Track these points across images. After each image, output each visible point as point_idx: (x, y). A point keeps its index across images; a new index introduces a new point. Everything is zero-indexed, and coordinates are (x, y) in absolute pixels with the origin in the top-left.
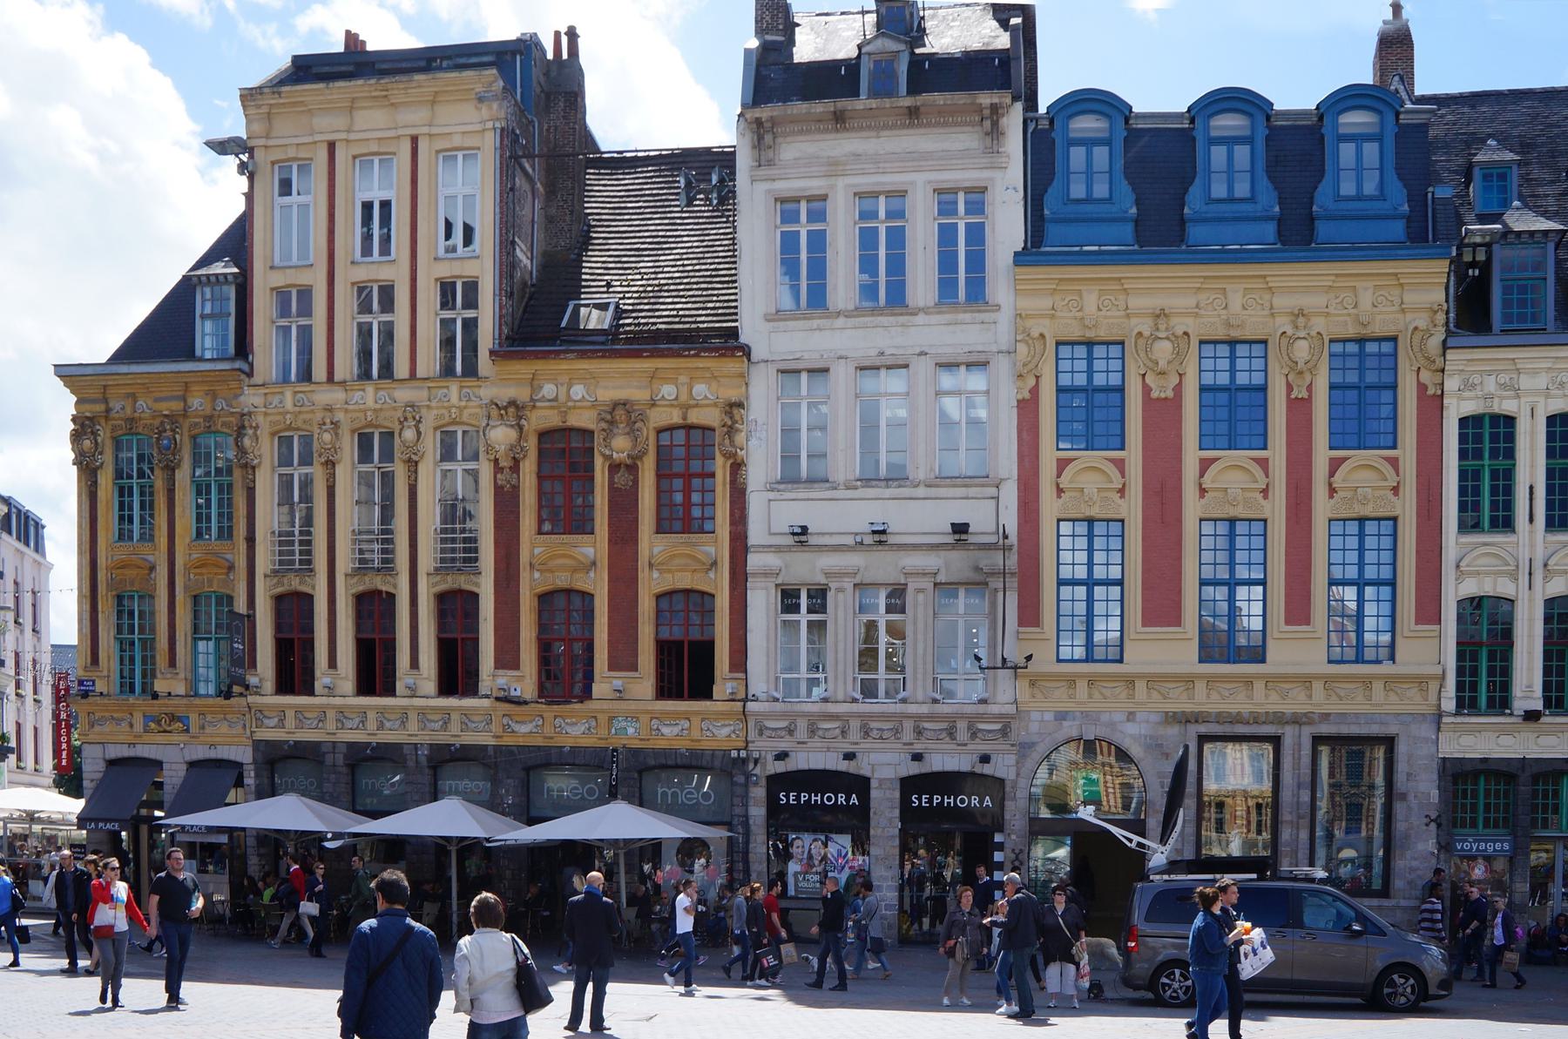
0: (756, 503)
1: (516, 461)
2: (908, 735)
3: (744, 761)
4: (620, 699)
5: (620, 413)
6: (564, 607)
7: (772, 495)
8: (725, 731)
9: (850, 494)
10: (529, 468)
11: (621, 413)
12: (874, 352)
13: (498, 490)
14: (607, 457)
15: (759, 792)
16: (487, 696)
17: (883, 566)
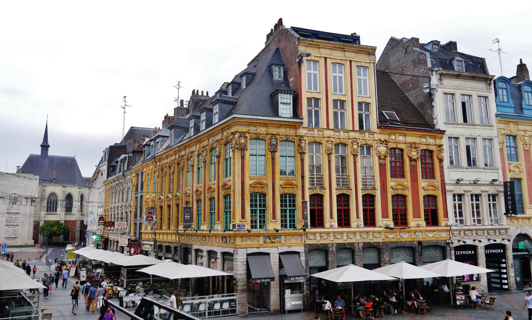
0: (446, 171)
1: (385, 157)
2: (486, 235)
3: (449, 243)
4: (418, 227)
5: (413, 145)
6: (400, 199)
7: (449, 170)
8: (445, 235)
9: (467, 170)
10: (388, 159)
11: (413, 146)
12: (469, 134)
13: (380, 165)
14: (409, 157)
15: (453, 252)
16: (380, 227)
17: (476, 190)
